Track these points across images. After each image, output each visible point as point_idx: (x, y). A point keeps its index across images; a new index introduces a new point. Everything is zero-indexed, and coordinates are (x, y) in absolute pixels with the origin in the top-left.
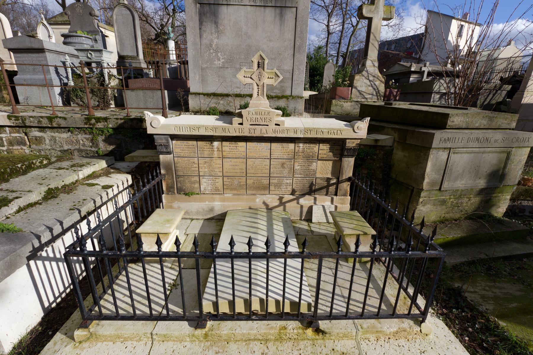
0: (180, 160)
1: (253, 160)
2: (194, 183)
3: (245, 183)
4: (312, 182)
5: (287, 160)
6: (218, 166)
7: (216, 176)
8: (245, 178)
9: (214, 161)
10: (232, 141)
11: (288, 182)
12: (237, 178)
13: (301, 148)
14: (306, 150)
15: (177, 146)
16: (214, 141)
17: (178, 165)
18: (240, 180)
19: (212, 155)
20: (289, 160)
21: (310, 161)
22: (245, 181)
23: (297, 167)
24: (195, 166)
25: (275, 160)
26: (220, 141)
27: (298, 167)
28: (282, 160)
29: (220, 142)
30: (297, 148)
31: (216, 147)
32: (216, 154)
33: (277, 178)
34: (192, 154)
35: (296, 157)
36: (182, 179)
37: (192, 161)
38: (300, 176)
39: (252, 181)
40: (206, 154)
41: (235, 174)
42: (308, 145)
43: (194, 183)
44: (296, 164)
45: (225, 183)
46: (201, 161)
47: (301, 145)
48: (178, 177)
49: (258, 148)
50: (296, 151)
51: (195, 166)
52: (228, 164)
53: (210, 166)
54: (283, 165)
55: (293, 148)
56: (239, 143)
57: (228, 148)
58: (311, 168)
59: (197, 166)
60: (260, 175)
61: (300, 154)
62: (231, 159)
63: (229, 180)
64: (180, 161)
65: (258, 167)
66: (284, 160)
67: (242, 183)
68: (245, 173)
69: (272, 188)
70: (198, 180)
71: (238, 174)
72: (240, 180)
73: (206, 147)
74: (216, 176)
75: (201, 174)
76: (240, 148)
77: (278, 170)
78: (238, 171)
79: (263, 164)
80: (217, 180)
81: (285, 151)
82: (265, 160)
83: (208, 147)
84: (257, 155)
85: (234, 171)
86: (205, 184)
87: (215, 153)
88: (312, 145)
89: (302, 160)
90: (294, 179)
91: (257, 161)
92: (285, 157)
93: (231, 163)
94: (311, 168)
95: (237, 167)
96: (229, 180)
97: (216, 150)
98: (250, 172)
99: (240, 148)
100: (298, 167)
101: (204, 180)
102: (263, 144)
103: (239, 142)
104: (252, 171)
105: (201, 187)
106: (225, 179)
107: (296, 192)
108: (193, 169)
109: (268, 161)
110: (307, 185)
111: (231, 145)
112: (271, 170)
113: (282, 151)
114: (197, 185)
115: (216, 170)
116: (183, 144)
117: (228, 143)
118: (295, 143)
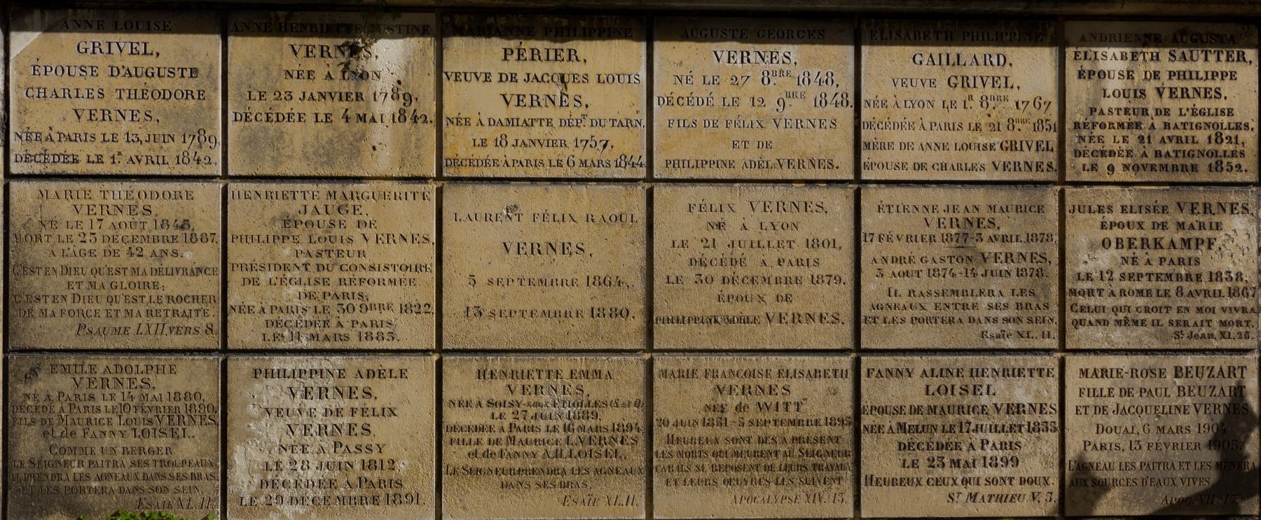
0: (61, 204)
1: (712, 194)
2: (174, 419)
3: (636, 416)
4: (1239, 391)
5: (1000, 197)
6: (401, 254)
7: (380, 353)
8: (633, 368)
9: (368, 209)
10: (529, 34)
11: (1022, 392)
12: (564, 364)
13: (1113, 84)
14: (1152, 102)
15: (51, 82)
16: (377, 32)
17: (37, 253)
18: (593, 390)
19: (355, 151)
20: (1018, 197)
21: (1200, 196)
22: (635, 391)
23: (1091, 256)
24: (190, 255)
25: (898, 195)
26: (423, 31)
27: (1106, 259)
28: (959, 197)
29: (428, 43)
30: (1075, 87)
31: (385, 84)
32: (384, 149)
33: (920, 363)
34: (173, 149)
35: (1076, 168)
36: (63, 383)
37: (166, 210)
38: (1119, 337)
39: (701, 391)
40: (299, 145)
41: (545, 333)
42: (1166, 61)
43: (174, 419)
44: (1083, 231)
45: (452, 416)
46: (251, 211)
47: (1112, 59)
48: (23, 364)
49: (753, 87)
50: (1075, 113)
51: (190, 255)
52: (482, 238)
53: (329, 251)
54: (965, 236)
55: (1048, 88)
56: (584, 48)
57: (496, 88)
58: (1210, 262)
59: (208, 254)
60: (767, 336)
61: (1111, 139)
62: (512, 194)
63: (498, 389)
64: (64, 209)
65: (753, 257)
66: (978, 197)
67: (609, 417)
68: (638, 321)
69: (881, 456)
70: (208, 388)
71: (577, 333)
72: (593, 390)
73: (297, 86)
74: (380, 353)
75: (244, 332)
76: (591, 93)
77: (922, 284)
78: (580, 298)
79: (800, 236)
80: (385, 393)
81: (976, 113)
82: (815, 195)
83: (320, 85)
84: (740, 156)
85: (536, 299)
86: (274, 431)
87: (381, 134)
88: (1204, 63)
89: (1129, 197)
90: (1075, 364)
91: (744, 212)
92: (985, 165)
93: (513, 231)
94: (1210, 262)
95: (565, 266)
96: (498, 389)
97: (388, 107)
98: (681, 308)
99: (591, 93)
100: (1106, 259)
101: (272, 392)
102: (795, 51)
103: (588, 35)
104: (701, 301)
105: (238, 456)
106: (460, 380)
107: (1102, 487)
108: (171, 286)
109: (839, 202)
110: (1195, 426)
111: (521, 69)
112: (870, 288)
113: (953, 116)
114: (194, 444)
115: (377, 294)
116: (101, 61)
117: (497, 45)
118: (1060, 43)
